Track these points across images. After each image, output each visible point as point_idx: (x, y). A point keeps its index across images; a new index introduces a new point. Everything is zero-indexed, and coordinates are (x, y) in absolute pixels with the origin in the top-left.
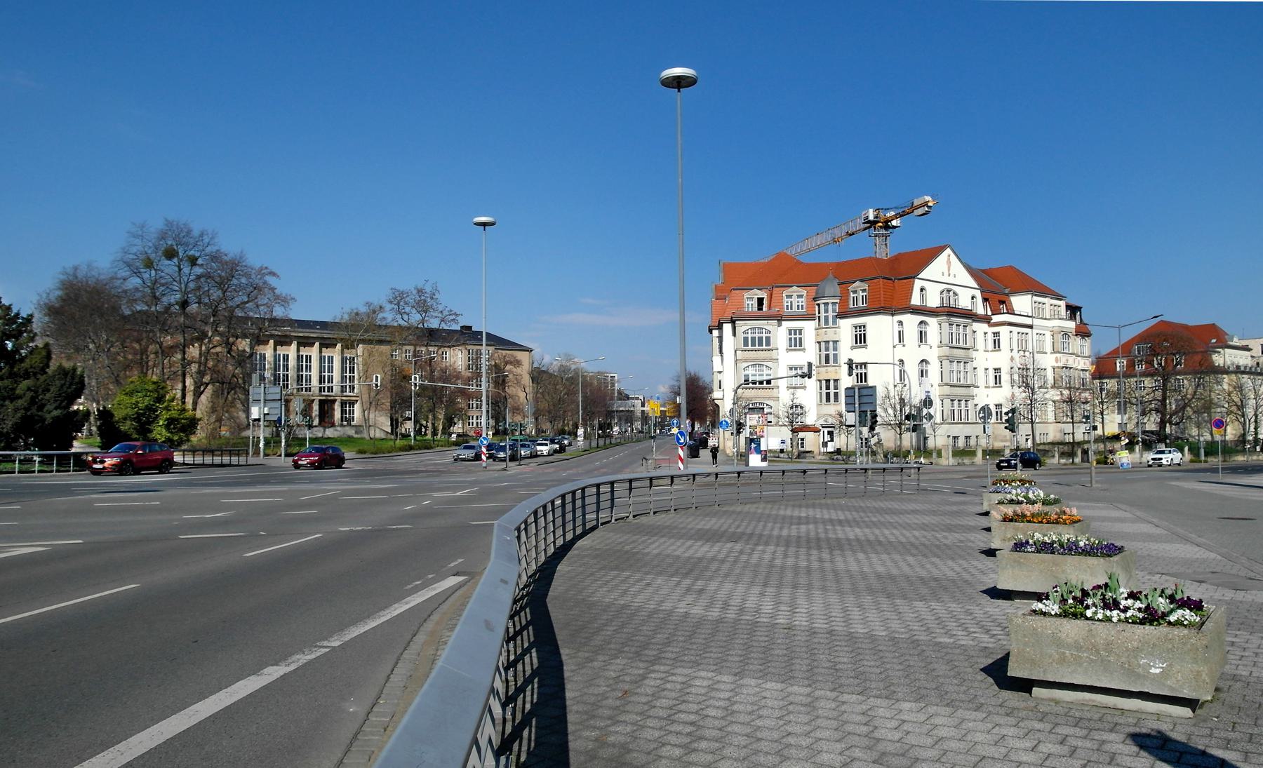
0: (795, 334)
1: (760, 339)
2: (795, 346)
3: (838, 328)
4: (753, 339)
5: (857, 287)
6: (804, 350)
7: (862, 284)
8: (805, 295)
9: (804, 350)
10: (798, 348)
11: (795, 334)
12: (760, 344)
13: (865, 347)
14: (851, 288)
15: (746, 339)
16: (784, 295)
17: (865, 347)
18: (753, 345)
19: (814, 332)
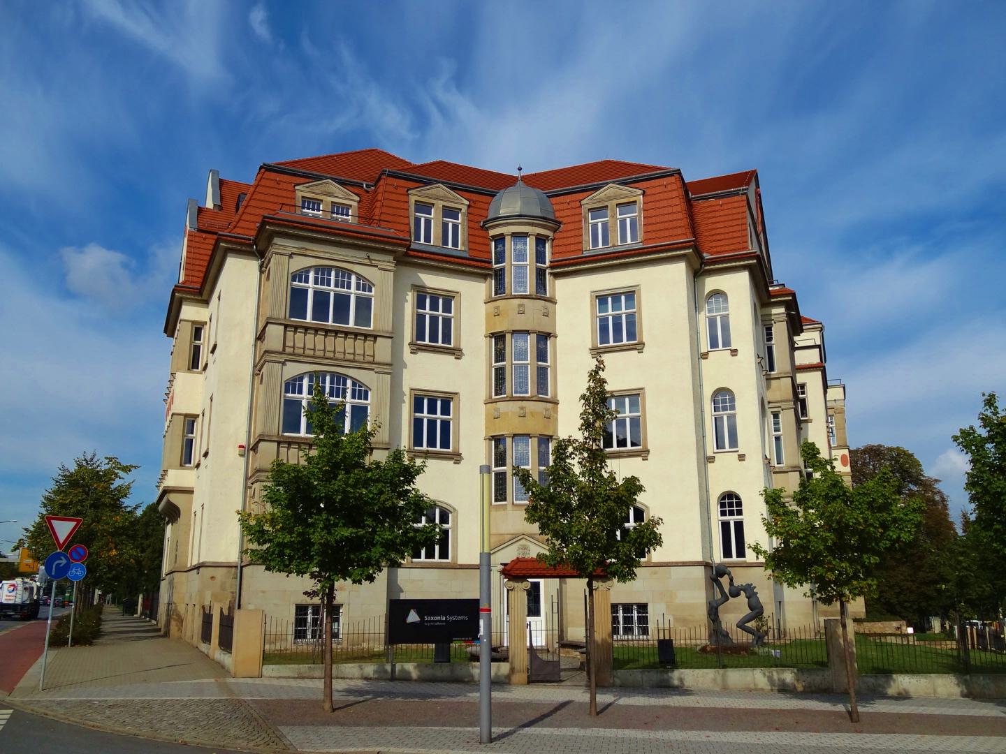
0: (434, 307)
1: (342, 301)
2: (434, 338)
3: (552, 301)
4: (321, 299)
5: (610, 199)
6: (457, 353)
7: (625, 190)
8: (464, 209)
9: (457, 353)
10: (440, 344)
11: (434, 307)
12: (342, 314)
13: (639, 347)
14: (588, 202)
15: (298, 297)
16: (412, 199)
17: (639, 347)
18: (320, 311)
19: (482, 310)
